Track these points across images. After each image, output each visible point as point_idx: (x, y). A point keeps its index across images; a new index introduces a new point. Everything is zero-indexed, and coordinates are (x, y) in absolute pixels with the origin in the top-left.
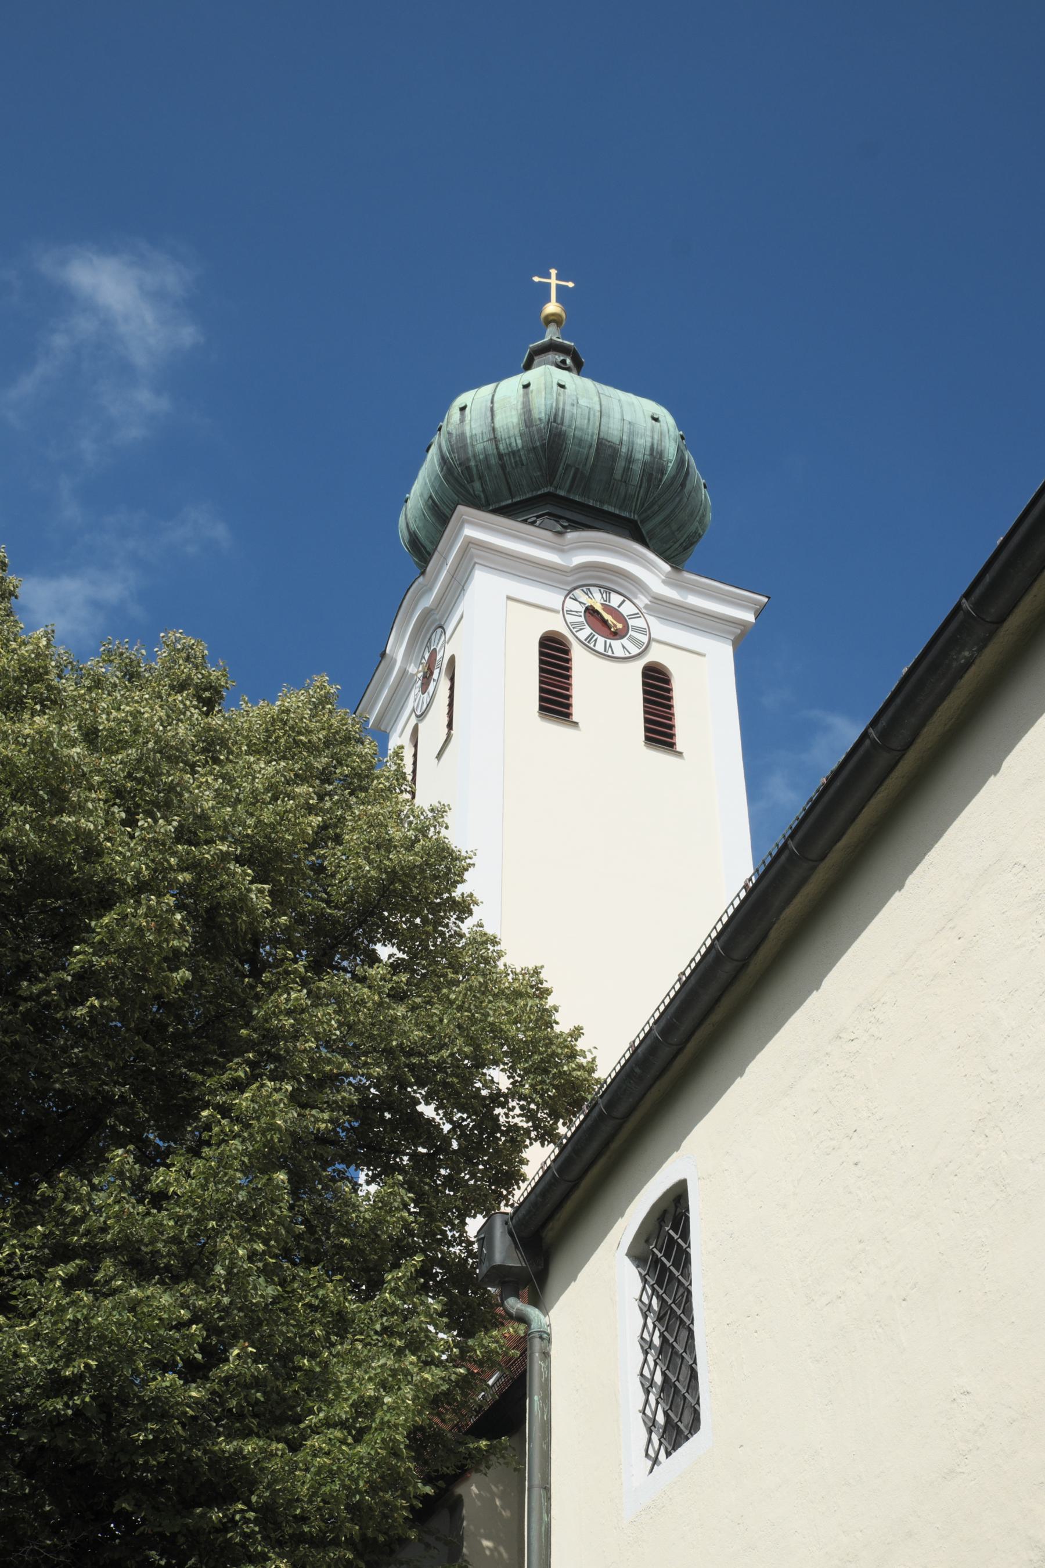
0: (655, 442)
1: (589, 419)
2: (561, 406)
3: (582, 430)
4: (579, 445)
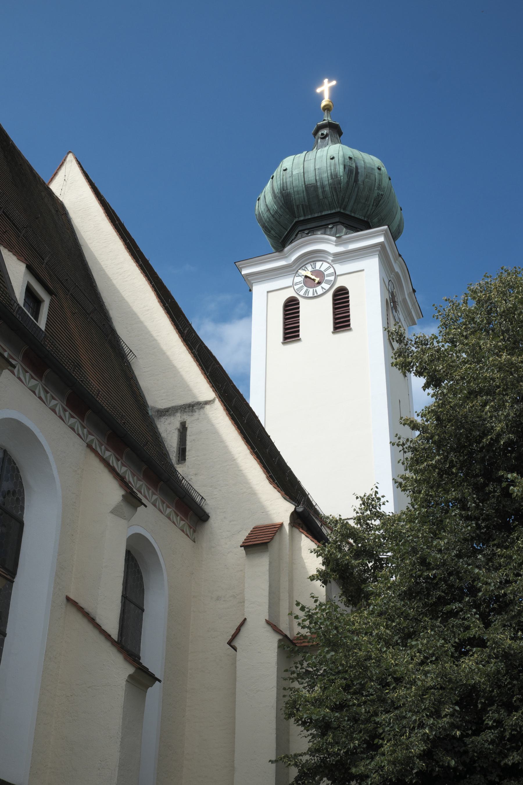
1: (299, 180)
2: (285, 181)
3: (297, 186)
4: (298, 194)
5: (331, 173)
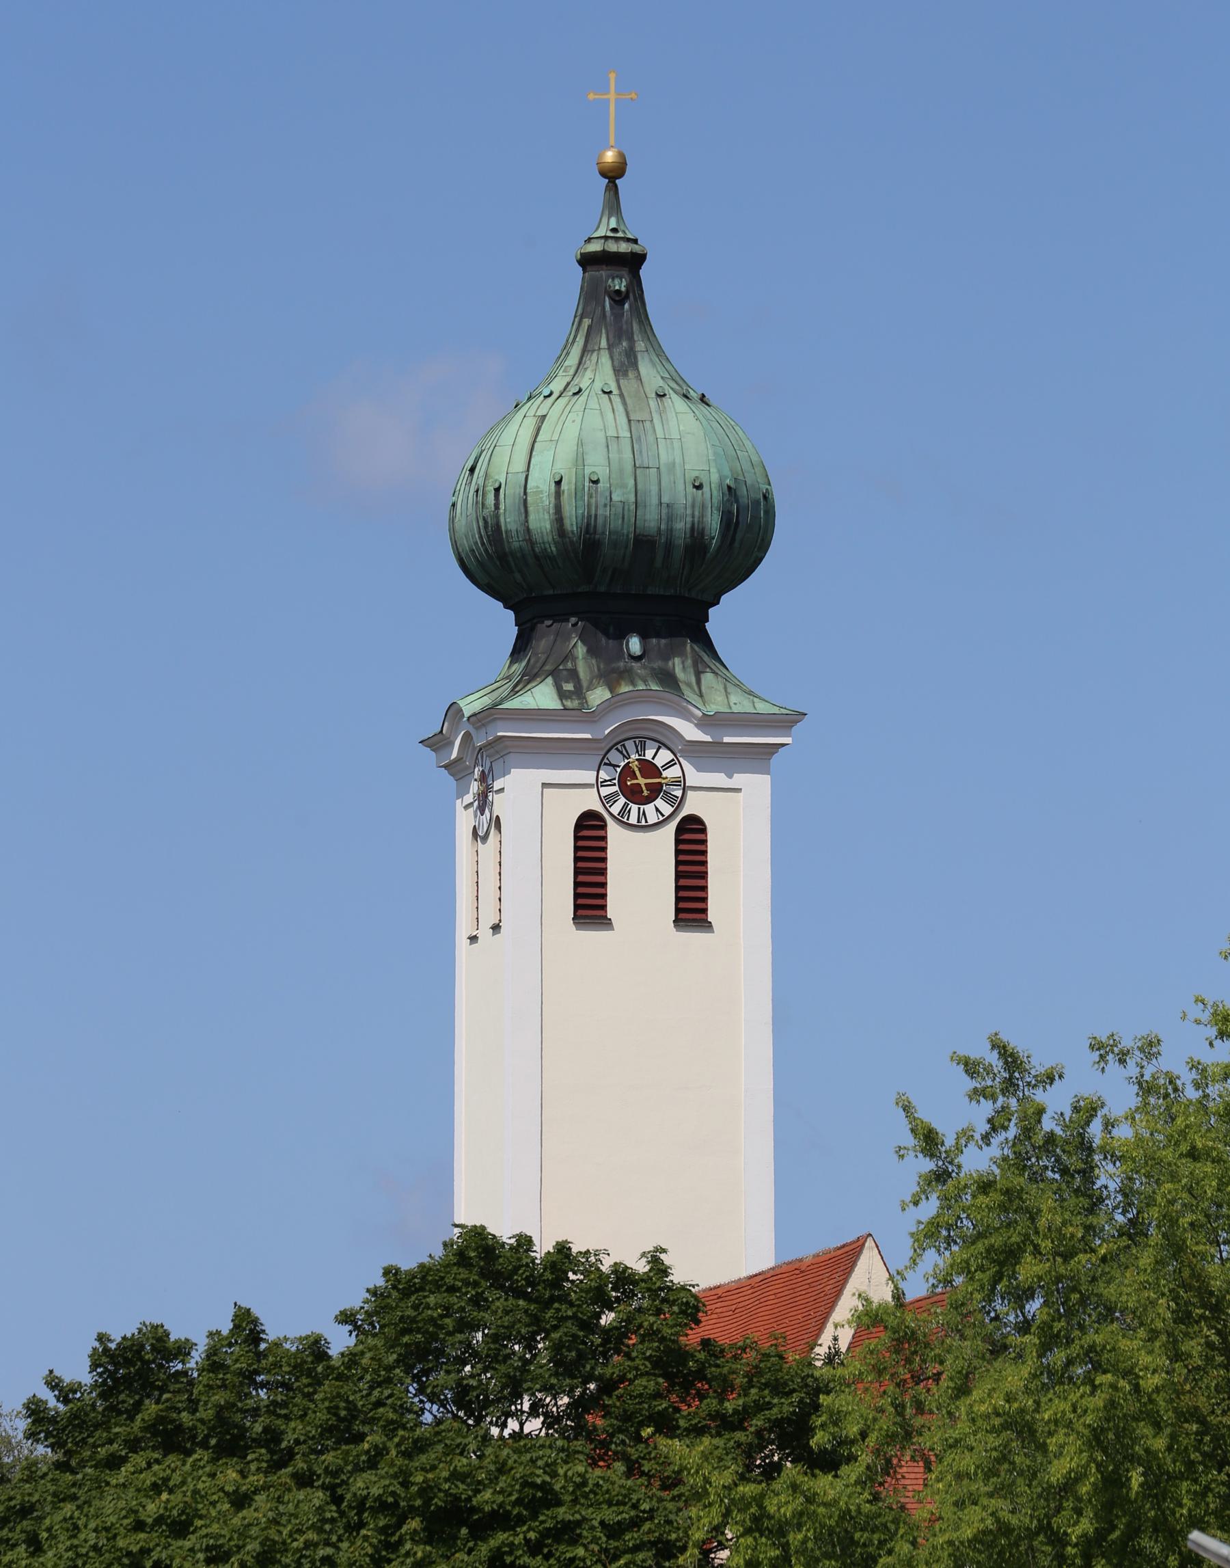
0: (696, 520)
1: (623, 518)
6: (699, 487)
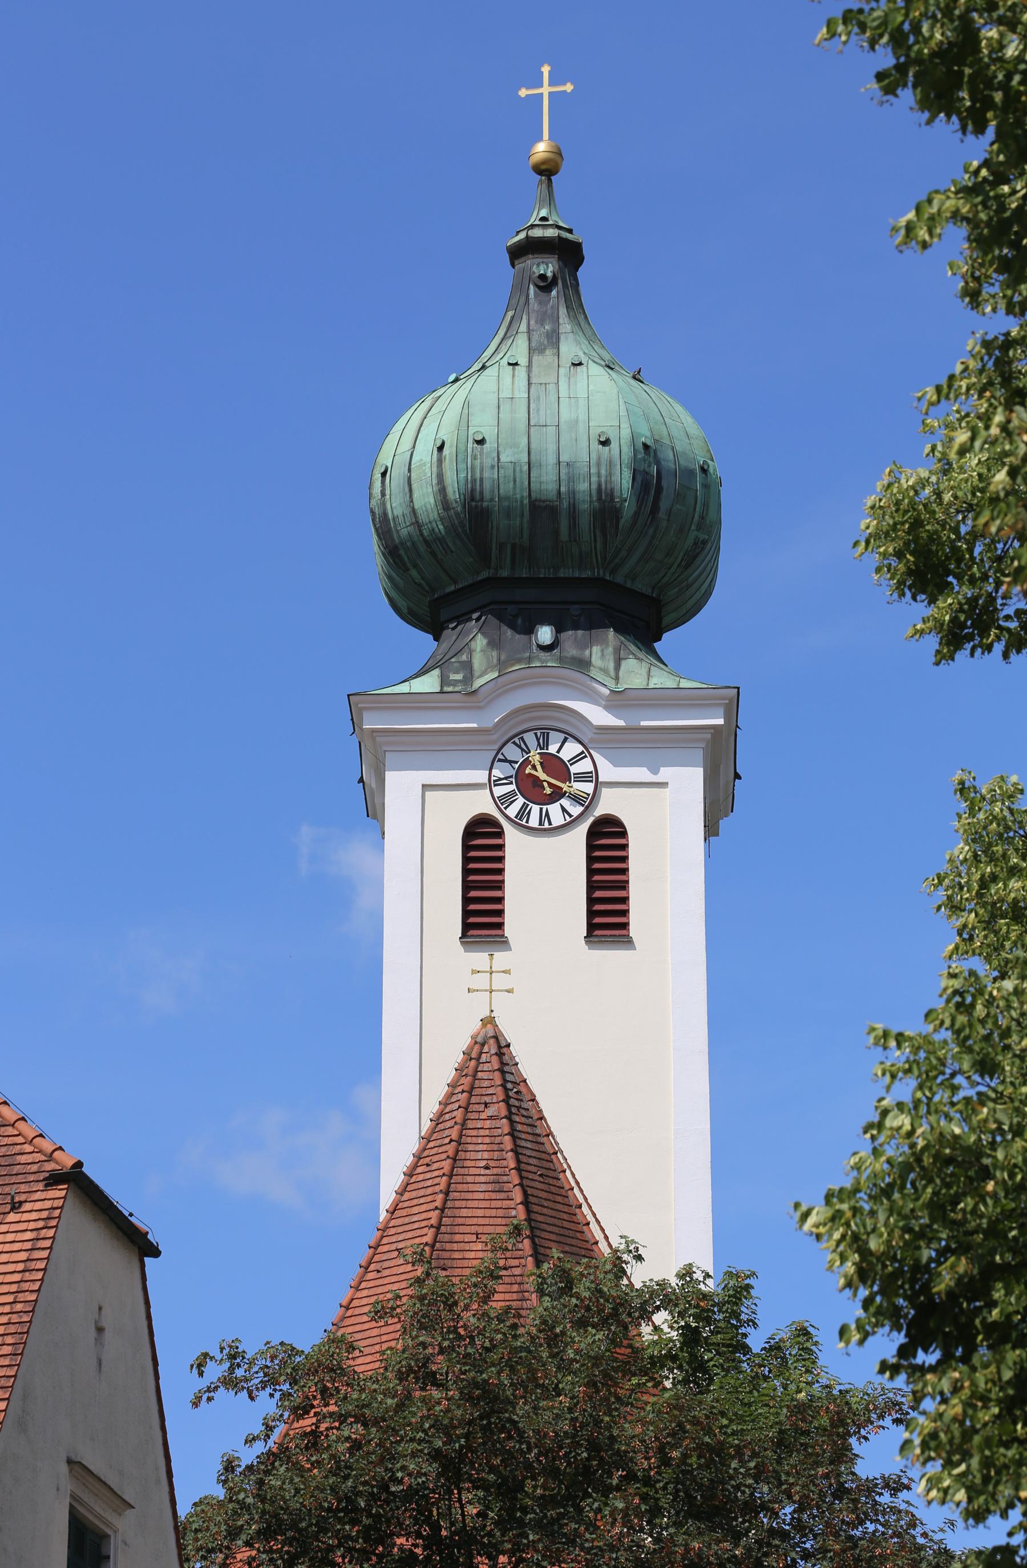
1: (515, 481)
2: (478, 476)
3: (507, 498)
5: (599, 485)
6: (606, 443)
